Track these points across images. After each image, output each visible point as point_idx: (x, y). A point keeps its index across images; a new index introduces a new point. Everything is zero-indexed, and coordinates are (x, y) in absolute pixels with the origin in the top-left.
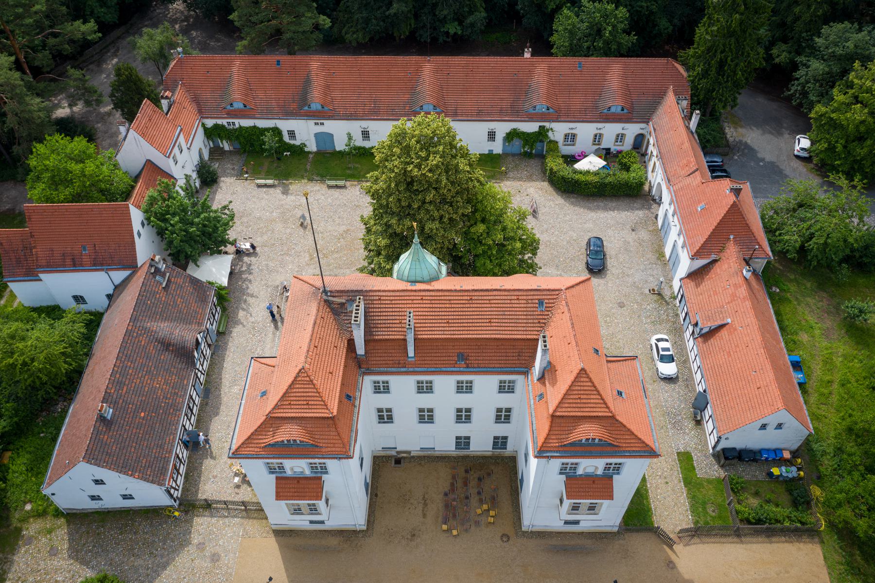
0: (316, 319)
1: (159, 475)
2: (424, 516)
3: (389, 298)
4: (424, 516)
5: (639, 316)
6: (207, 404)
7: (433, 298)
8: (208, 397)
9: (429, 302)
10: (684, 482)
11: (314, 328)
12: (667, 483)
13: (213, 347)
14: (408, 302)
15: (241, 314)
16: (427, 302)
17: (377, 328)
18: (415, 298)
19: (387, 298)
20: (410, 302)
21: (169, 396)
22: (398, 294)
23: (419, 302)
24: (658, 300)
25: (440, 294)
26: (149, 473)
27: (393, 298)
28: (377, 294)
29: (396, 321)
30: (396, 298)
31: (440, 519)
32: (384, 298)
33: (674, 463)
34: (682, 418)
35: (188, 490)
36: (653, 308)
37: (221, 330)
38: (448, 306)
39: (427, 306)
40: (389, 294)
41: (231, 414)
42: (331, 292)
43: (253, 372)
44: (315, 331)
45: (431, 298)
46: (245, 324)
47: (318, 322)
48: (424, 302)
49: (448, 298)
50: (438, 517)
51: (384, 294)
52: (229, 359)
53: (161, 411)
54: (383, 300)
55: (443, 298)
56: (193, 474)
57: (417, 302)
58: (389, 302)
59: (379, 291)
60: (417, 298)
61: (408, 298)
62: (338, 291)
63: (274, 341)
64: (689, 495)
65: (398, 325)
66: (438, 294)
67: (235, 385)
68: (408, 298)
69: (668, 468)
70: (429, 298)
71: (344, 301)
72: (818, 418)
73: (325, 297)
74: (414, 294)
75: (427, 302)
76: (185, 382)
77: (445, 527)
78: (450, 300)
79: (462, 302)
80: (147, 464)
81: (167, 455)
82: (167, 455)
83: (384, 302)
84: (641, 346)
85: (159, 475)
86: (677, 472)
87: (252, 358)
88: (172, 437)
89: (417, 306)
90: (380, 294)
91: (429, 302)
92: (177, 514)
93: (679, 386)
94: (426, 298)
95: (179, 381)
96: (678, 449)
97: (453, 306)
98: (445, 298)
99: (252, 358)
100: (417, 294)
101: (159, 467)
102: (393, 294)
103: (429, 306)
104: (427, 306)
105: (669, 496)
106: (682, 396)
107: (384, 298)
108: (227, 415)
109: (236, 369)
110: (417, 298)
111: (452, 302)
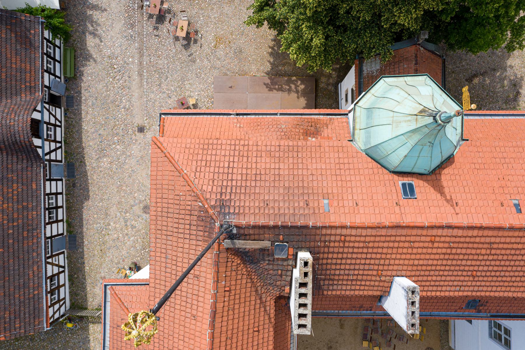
0: (215, 303)
1: (32, 321)
2: (342, 326)
3: (363, 239)
4: (342, 326)
6: (74, 185)
7: (457, 240)
8: (74, 176)
9: (446, 245)
11: (213, 326)
13: (64, 101)
14: (401, 244)
15: (91, 42)
16: (441, 245)
17: (333, 280)
18: (418, 239)
19: (358, 239)
20: (406, 245)
21: (16, 216)
22: (383, 232)
23: (426, 245)
25: (475, 232)
26: (17, 326)
27: (372, 239)
28: (339, 231)
29: (370, 273)
30: (378, 239)
31: (360, 331)
32: (353, 239)
35: (76, 295)
37: (68, 75)
38: (483, 252)
39: (439, 251)
40: (364, 232)
41: (106, 197)
42: (238, 227)
43: (112, 320)
44: (217, 331)
45: (453, 239)
46: (99, 59)
47: (220, 305)
48: (436, 245)
49: (488, 240)
50: (356, 328)
51: (354, 232)
52: (89, 117)
53: (11, 241)
54: (350, 241)
55: (478, 240)
56: (78, 276)
57: (421, 245)
58: (361, 245)
59: (343, 227)
60: (423, 239)
61: (403, 239)
62: (254, 227)
63: (142, 86)
65: (374, 278)
66: (470, 233)
67: (105, 156)
68: (403, 239)
70: (448, 239)
71: (266, 244)
73: (227, 244)
74: (419, 232)
75: (441, 245)
76: (34, 186)
77: (365, 344)
78: (490, 243)
79: (515, 246)
80: (12, 316)
81: (36, 292)
82: (36, 292)
83: (351, 245)
85: (32, 321)
87: (106, 286)
88: (35, 268)
89: (420, 251)
90: (344, 232)
91: (446, 245)
92: (70, 325)
94: (443, 239)
95: (25, 188)
97: (493, 252)
98: (483, 240)
99: (106, 286)
100: (424, 232)
101: (29, 312)
102: (374, 232)
103: (444, 251)
104: (439, 251)
107: (353, 239)
108: (102, 200)
109: (101, 132)
110: (423, 239)
111: (495, 246)
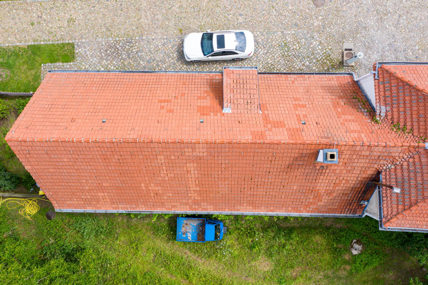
5: (296, 25)
10: (34, 46)
12: (32, 24)
24: (331, 61)
33: (59, 37)
34: (124, 60)
36: (313, 49)
64: (17, 48)
69: (51, 28)
72: (132, 243)
84: (241, 20)
86: (47, 38)
93: (174, 64)
96: (78, 46)
105: (16, 24)
106: (158, 65)
